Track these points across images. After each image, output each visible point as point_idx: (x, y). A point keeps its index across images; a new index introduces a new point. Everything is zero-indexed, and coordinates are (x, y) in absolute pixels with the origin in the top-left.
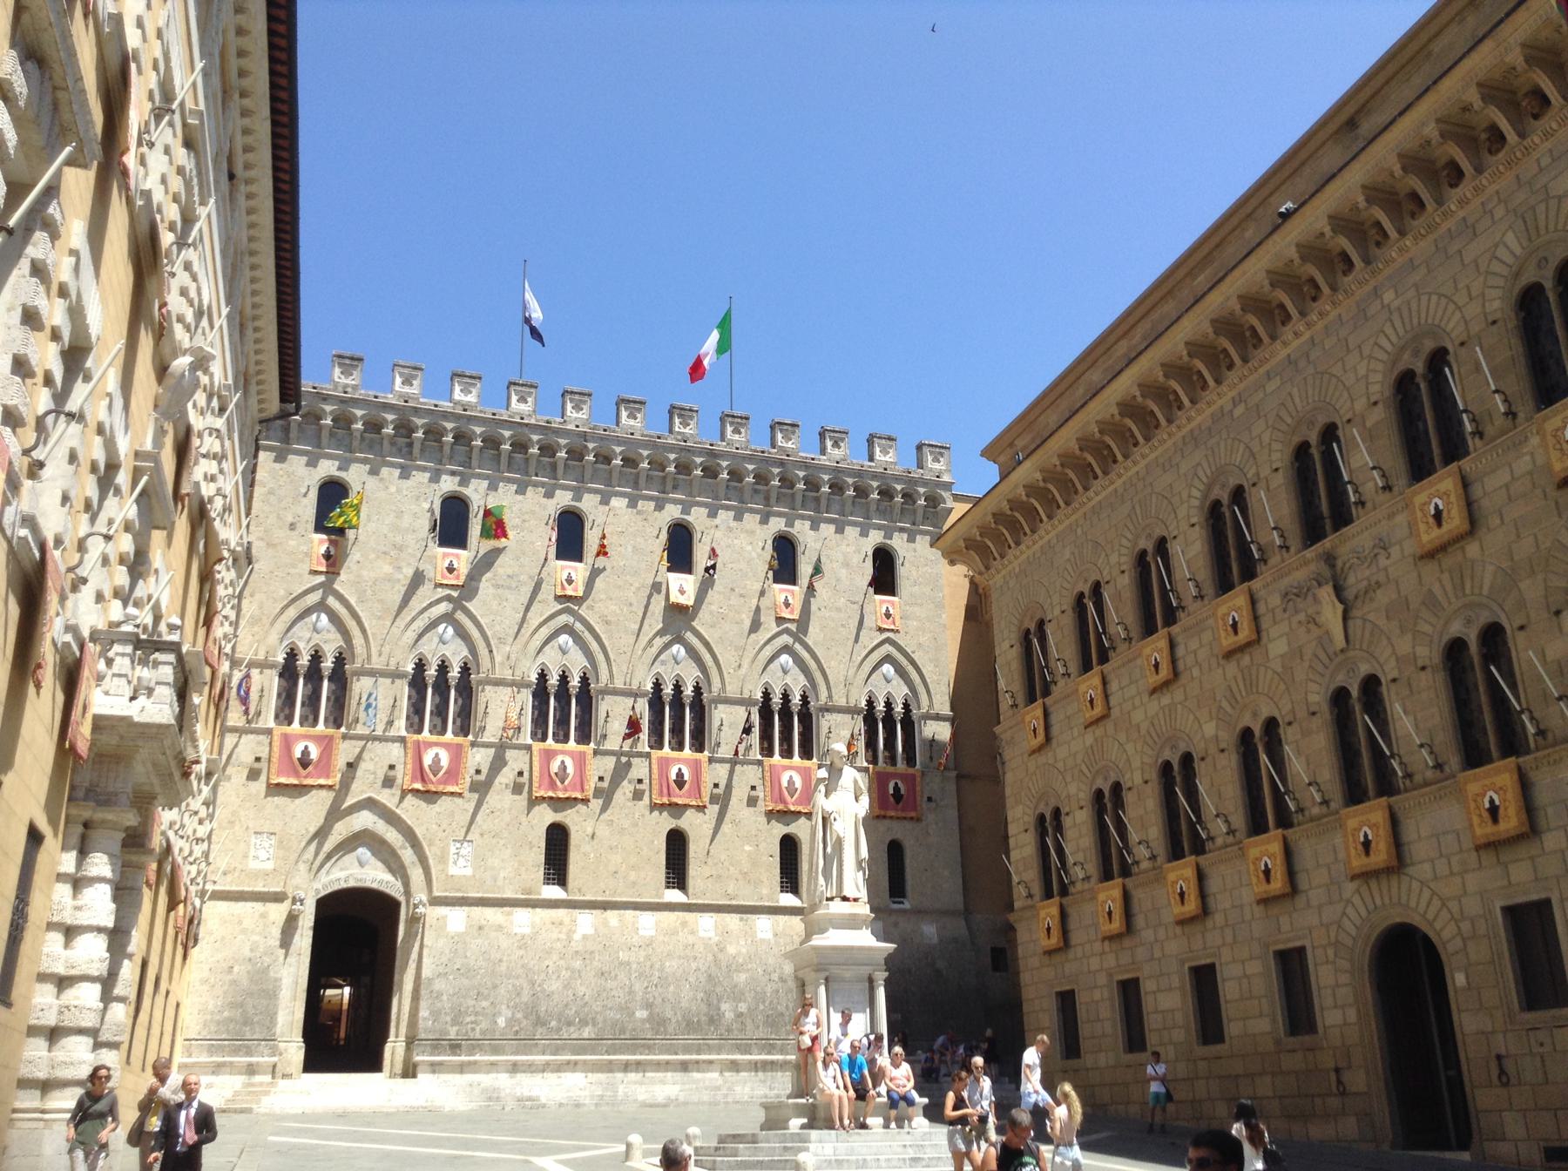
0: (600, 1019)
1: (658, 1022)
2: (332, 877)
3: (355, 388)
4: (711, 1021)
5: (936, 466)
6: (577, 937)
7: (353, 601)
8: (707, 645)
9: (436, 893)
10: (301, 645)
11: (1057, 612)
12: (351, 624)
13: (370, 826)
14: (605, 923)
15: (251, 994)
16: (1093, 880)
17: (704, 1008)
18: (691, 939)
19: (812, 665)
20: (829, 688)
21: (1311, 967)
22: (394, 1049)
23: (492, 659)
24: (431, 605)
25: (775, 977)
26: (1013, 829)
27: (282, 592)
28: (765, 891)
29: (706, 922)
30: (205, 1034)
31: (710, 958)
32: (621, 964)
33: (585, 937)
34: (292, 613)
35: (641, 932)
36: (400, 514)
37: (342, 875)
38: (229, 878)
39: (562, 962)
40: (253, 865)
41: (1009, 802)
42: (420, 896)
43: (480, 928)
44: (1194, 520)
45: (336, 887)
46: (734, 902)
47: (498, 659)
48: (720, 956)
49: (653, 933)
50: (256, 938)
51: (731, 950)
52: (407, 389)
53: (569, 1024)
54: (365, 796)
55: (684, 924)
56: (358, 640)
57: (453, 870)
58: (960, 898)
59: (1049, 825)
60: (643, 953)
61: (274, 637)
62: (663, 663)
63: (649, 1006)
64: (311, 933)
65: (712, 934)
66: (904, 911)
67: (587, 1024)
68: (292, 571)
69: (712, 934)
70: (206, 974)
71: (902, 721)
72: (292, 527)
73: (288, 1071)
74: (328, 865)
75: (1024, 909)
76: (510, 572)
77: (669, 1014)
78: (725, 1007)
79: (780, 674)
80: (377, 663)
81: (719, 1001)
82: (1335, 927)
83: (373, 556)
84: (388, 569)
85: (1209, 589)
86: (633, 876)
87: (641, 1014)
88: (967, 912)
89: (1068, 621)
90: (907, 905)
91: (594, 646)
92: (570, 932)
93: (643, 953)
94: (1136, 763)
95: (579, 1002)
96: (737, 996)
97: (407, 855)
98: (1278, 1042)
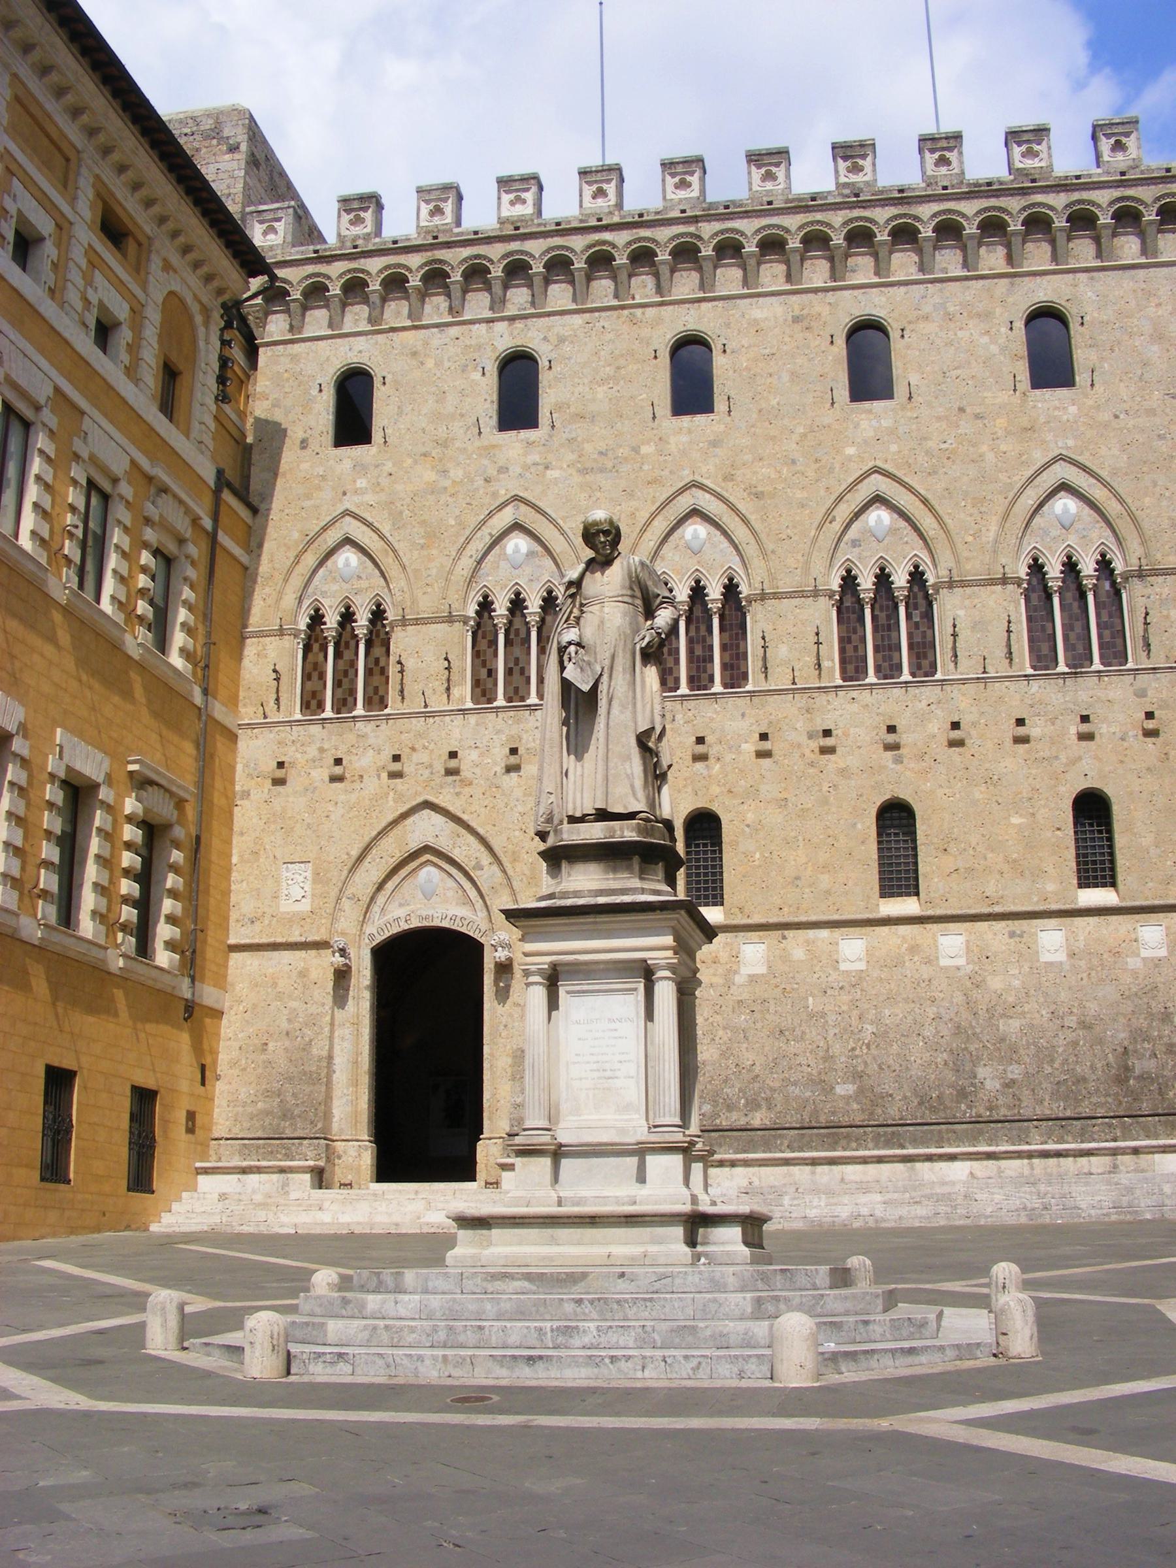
0: (778, 1098)
1: (869, 1095)
2: (389, 917)
3: (367, 237)
6: (738, 979)
7: (386, 529)
8: (925, 502)
12: (387, 561)
13: (431, 842)
14: (785, 958)
15: (290, 1079)
17: (951, 1077)
18: (926, 972)
19: (1112, 508)
20: (1144, 542)
22: (487, 1152)
24: (490, 515)
25: (1071, 1021)
27: (296, 535)
28: (1051, 887)
29: (951, 944)
31: (959, 998)
32: (811, 1016)
33: (753, 979)
34: (310, 560)
35: (843, 966)
37: (401, 912)
38: (258, 926)
39: (718, 1018)
45: (395, 930)
46: (997, 909)
48: (975, 994)
49: (861, 966)
50: (293, 1004)
51: (996, 983)
52: (437, 220)
53: (730, 1108)
54: (420, 799)
55: (914, 949)
60: (845, 998)
61: (289, 599)
62: (855, 543)
63: (857, 1076)
64: (367, 995)
67: (759, 1106)
69: (961, 962)
70: (235, 1054)
72: (304, 444)
73: (349, 1178)
74: (381, 899)
76: (602, 446)
77: (889, 1087)
78: (982, 1072)
79: (1055, 532)
81: (976, 1061)
83: (409, 461)
84: (430, 476)
87: (845, 1089)
91: (740, 533)
92: (731, 972)
93: (845, 998)
95: (746, 1075)
96: (1007, 1051)
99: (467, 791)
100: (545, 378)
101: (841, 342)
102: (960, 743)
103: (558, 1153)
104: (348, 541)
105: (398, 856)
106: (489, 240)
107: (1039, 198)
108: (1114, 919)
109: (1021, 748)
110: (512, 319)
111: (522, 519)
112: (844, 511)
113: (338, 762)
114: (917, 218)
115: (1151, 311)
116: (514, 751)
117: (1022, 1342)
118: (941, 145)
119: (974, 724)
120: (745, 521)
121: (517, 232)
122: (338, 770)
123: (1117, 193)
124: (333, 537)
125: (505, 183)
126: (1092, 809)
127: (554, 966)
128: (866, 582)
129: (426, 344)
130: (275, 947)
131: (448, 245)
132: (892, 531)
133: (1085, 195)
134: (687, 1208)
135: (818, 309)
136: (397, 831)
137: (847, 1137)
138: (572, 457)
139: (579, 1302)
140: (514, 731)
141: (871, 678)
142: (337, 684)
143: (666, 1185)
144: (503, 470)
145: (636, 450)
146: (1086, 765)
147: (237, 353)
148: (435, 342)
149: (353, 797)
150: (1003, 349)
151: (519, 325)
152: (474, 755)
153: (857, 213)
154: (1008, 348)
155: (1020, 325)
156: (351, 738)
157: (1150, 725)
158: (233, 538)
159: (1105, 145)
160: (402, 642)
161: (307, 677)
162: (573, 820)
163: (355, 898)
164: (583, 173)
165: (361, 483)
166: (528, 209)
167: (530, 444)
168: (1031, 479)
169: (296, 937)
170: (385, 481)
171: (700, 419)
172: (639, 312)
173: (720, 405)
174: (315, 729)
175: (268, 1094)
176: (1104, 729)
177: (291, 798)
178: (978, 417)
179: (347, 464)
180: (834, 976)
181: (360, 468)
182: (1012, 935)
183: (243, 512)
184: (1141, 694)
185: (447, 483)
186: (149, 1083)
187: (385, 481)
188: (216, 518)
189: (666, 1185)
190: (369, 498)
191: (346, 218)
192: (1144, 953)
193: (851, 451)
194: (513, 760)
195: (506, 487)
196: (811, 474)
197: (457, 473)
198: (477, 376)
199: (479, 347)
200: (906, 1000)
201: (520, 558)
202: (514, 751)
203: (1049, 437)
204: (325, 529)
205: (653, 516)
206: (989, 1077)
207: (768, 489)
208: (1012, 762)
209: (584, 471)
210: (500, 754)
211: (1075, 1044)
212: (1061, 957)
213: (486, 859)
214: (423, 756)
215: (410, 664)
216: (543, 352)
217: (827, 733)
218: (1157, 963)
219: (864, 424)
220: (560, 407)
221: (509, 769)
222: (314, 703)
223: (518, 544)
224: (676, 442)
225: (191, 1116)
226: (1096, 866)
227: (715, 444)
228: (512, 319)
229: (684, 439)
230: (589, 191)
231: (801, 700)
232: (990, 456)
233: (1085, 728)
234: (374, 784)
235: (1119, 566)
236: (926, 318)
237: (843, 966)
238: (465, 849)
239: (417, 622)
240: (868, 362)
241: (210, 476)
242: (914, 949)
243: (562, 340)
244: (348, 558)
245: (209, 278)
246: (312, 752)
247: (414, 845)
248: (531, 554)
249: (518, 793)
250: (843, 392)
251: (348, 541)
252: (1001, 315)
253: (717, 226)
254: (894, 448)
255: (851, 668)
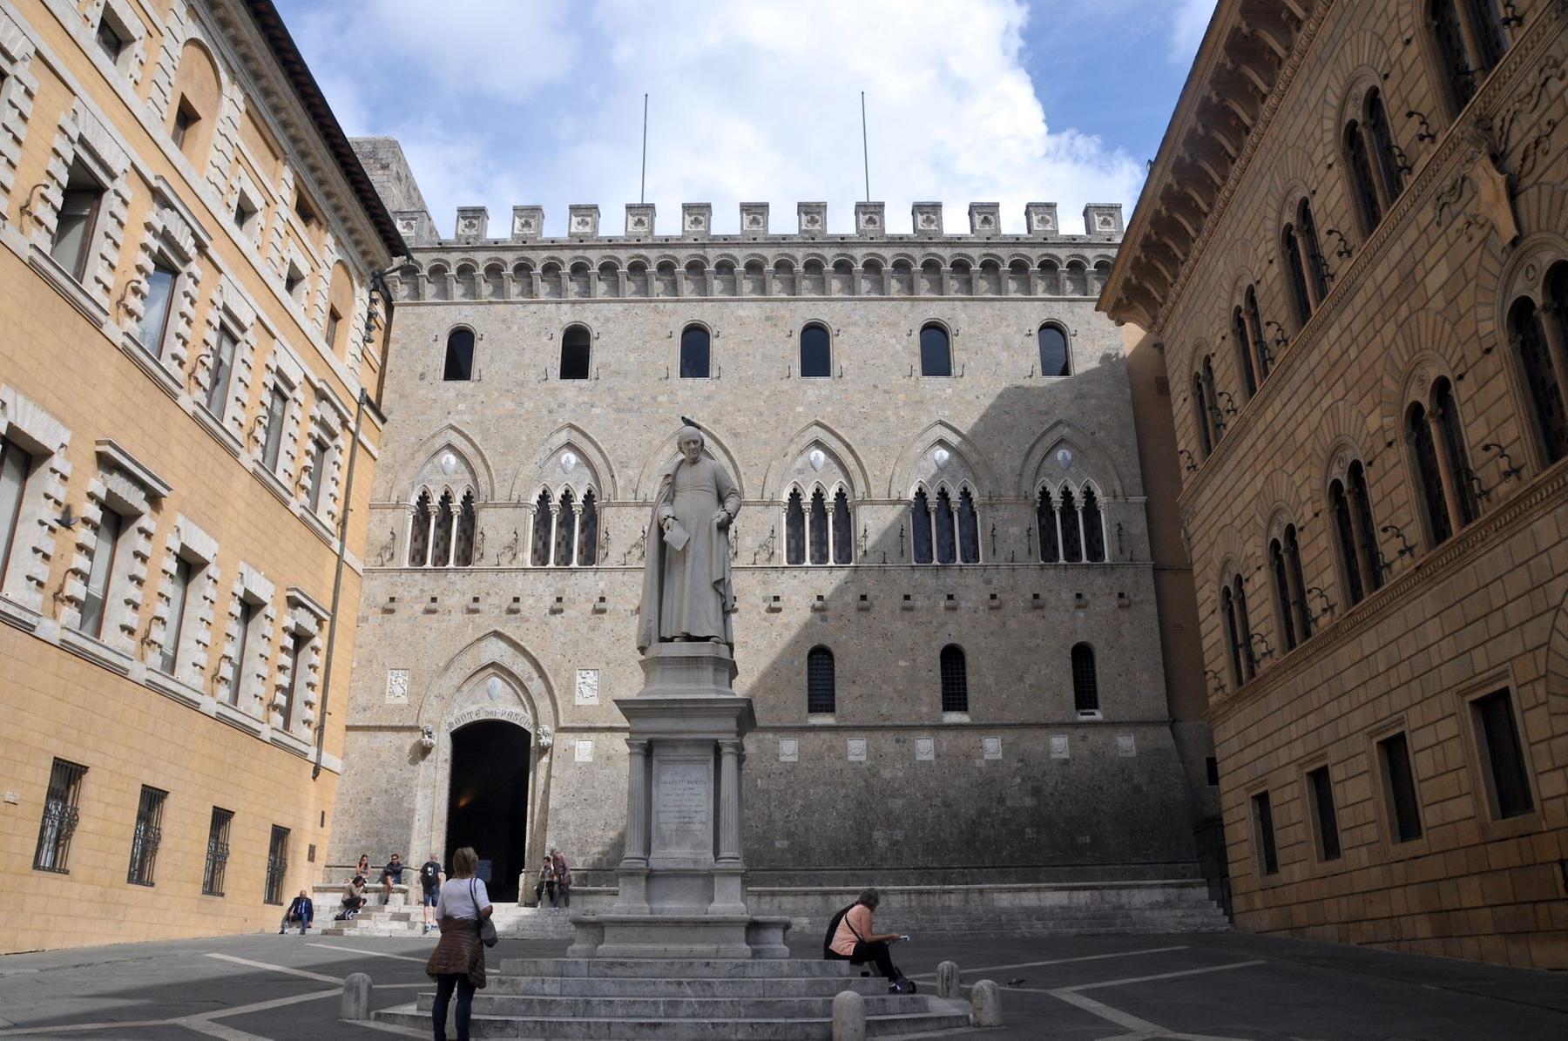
2: (465, 711)
3: (477, 237)
4: (862, 850)
5: (1107, 229)
8: (848, 446)
9: (562, 724)
10: (431, 488)
11: (1219, 340)
12: (477, 463)
13: (497, 659)
16: (1276, 654)
18: (839, 765)
19: (973, 457)
21: (1517, 714)
23: (614, 484)
25: (937, 801)
26: (1203, 612)
28: (924, 710)
29: (857, 747)
30: (344, 862)
31: (861, 783)
35: (782, 759)
36: (521, 351)
37: (473, 708)
38: (368, 713)
40: (389, 700)
41: (1198, 582)
42: (547, 727)
43: (608, 758)
44: (1330, 161)
45: (468, 721)
46: (888, 723)
47: (620, 483)
48: (874, 781)
50: (392, 770)
52: (526, 231)
55: (831, 748)
56: (483, 479)
57: (579, 701)
58: (1162, 704)
59: (1234, 600)
61: (404, 483)
63: (789, 835)
65: (863, 758)
66: (1095, 724)
68: (422, 418)
69: (863, 758)
71: (1085, 512)
72: (422, 376)
75: (1222, 703)
76: (631, 394)
78: (877, 834)
80: (501, 495)
82: (1544, 649)
85: (1354, 238)
86: (771, 699)
88: (1173, 722)
89: (1230, 342)
90: (1099, 716)
94: (1305, 494)
97: (536, 686)
98: (1484, 829)
99: (525, 625)
100: (595, 346)
101: (797, 336)
102: (867, 609)
103: (651, 876)
104: (450, 447)
105: (474, 668)
106: (562, 247)
107: (933, 250)
108: (966, 733)
109: (907, 615)
110: (574, 303)
111: (573, 440)
112: (793, 449)
113: (434, 600)
114: (852, 257)
115: (1003, 329)
116: (559, 600)
117: (990, 1016)
118: (871, 211)
119: (876, 597)
120: (726, 452)
121: (580, 243)
122: (433, 606)
123: (985, 251)
124: (440, 442)
125: (575, 209)
126: (952, 658)
127: (650, 742)
128: (807, 498)
129: (513, 314)
130: (380, 728)
131: (533, 248)
132: (826, 465)
133: (963, 251)
134: (747, 917)
135: (783, 312)
136: (473, 651)
137: (783, 877)
138: (610, 400)
139: (680, 983)
140: (560, 585)
141: (808, 563)
142: (436, 545)
143: (729, 902)
144: (562, 405)
145: (654, 398)
146: (951, 628)
147: (380, 308)
148: (520, 314)
149: (443, 625)
150: (905, 348)
151: (578, 307)
152: (531, 601)
153: (812, 250)
154: (909, 350)
155: (916, 333)
156: (444, 583)
157: (995, 603)
158: (369, 438)
159: (978, 219)
160: (486, 520)
161: (415, 539)
162: (663, 640)
163: (440, 697)
164: (629, 208)
165: (461, 407)
166: (588, 229)
167: (581, 389)
168: (920, 435)
169: (396, 722)
170: (478, 407)
171: (700, 381)
172: (661, 305)
173: (714, 372)
174: (418, 576)
175: (369, 835)
176: (963, 604)
177: (398, 623)
178: (886, 392)
179: (452, 393)
180: (776, 765)
181: (460, 396)
182: (898, 741)
183: (377, 421)
184: (988, 582)
185: (522, 411)
186: (284, 823)
187: (478, 407)
188: (358, 423)
189: (729, 902)
190: (467, 418)
191: (462, 223)
192: (987, 757)
193: (800, 409)
194: (558, 606)
195: (564, 417)
196: (772, 422)
197: (529, 405)
198: (545, 339)
199: (550, 320)
200: (825, 784)
201: (571, 467)
202: (559, 600)
203: (933, 408)
204: (433, 436)
205: (663, 444)
206: (880, 837)
207: (743, 431)
208: (898, 626)
209: (618, 410)
210: (549, 601)
211: (939, 817)
212: (931, 757)
213: (535, 675)
214: (496, 600)
215: (488, 534)
216: (594, 327)
217: (777, 598)
218: (995, 763)
219: (810, 392)
220: (605, 365)
221: (554, 612)
222: (418, 558)
223: (570, 458)
224: (682, 395)
225: (312, 849)
226: (954, 696)
227: (708, 398)
228: (574, 303)
229: (688, 393)
230: (632, 221)
231: (759, 575)
232: (893, 419)
233: (950, 603)
234: (458, 617)
235: (975, 495)
236: (855, 324)
237: (782, 759)
238: (521, 667)
239: (496, 506)
240: (816, 352)
241: (357, 395)
242: (831, 748)
243: (607, 320)
244: (450, 459)
245: (364, 254)
246: (415, 591)
247: (485, 662)
248: (577, 464)
249: (561, 629)
250: (797, 370)
251: (450, 447)
252: (904, 326)
253: (719, 252)
254: (829, 409)
255: (793, 555)
